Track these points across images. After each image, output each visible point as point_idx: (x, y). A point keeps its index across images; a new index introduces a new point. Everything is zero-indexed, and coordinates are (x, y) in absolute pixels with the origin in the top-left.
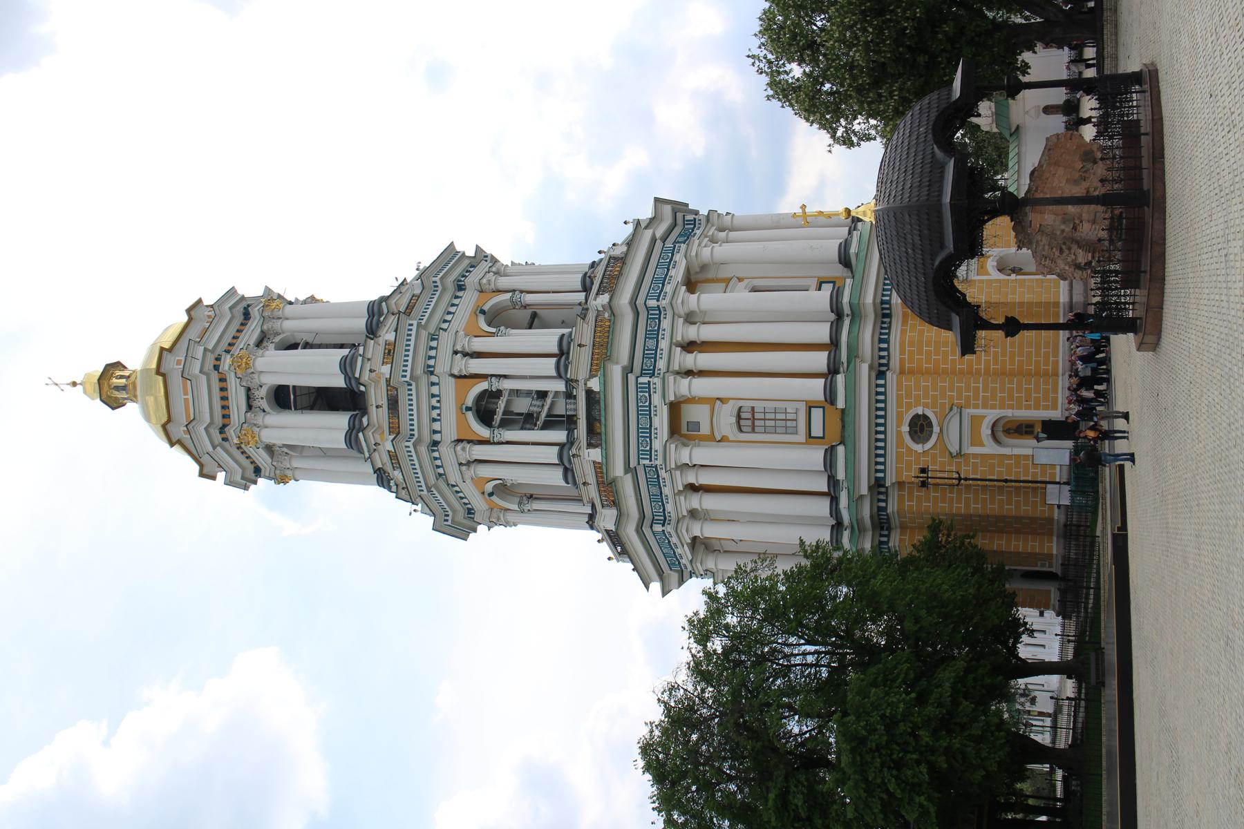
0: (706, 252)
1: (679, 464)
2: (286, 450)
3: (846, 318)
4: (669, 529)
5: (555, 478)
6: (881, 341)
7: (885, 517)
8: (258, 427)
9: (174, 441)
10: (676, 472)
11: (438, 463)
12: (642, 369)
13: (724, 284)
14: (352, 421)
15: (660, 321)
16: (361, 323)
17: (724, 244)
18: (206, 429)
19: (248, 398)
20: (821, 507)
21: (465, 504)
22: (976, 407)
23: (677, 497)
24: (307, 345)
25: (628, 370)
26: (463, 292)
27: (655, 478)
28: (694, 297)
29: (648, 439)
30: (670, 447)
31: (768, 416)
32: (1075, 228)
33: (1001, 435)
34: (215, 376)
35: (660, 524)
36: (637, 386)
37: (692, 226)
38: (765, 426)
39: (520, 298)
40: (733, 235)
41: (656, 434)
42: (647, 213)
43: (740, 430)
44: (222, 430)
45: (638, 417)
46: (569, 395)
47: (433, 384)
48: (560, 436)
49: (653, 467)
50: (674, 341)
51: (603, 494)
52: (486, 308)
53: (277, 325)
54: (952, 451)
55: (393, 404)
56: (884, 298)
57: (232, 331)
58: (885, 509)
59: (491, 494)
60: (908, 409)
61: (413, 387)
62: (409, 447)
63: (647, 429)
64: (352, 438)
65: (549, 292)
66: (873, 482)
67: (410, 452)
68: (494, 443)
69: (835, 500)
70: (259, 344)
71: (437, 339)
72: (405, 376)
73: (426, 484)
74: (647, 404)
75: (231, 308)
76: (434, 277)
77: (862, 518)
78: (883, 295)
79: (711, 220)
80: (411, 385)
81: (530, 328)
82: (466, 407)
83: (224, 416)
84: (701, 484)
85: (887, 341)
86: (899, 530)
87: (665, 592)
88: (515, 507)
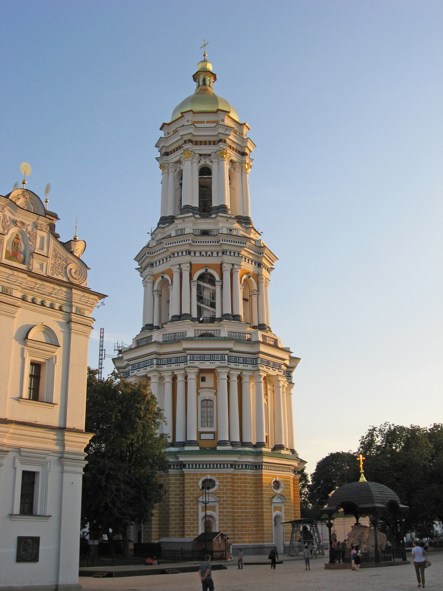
1: (188, 373)
2: (178, 170)
3: (255, 449)
4: (155, 367)
5: (174, 311)
6: (246, 465)
8: (192, 160)
10: (184, 372)
11: (180, 254)
18: (191, 133)
19: (205, 155)
21: (156, 263)
22: (219, 508)
23: (171, 371)
25: (231, 350)
26: (257, 266)
27: (179, 361)
29: (199, 359)
32: (364, 543)
35: (157, 363)
36: (224, 354)
39: (255, 294)
41: (202, 363)
44: (190, 141)
46: (213, 320)
47: (218, 253)
48: (195, 314)
49: (185, 360)
50: (243, 371)
51: (170, 335)
52: (251, 278)
54: (200, 498)
59: (162, 277)
60: (217, 478)
61: (217, 244)
62: (189, 240)
63: (204, 359)
64: (188, 208)
66: (184, 463)
69: (173, 444)
72: (222, 241)
73: (169, 247)
74: (215, 359)
80: (218, 243)
83: (196, 142)
85: (246, 468)
88: (155, 288)
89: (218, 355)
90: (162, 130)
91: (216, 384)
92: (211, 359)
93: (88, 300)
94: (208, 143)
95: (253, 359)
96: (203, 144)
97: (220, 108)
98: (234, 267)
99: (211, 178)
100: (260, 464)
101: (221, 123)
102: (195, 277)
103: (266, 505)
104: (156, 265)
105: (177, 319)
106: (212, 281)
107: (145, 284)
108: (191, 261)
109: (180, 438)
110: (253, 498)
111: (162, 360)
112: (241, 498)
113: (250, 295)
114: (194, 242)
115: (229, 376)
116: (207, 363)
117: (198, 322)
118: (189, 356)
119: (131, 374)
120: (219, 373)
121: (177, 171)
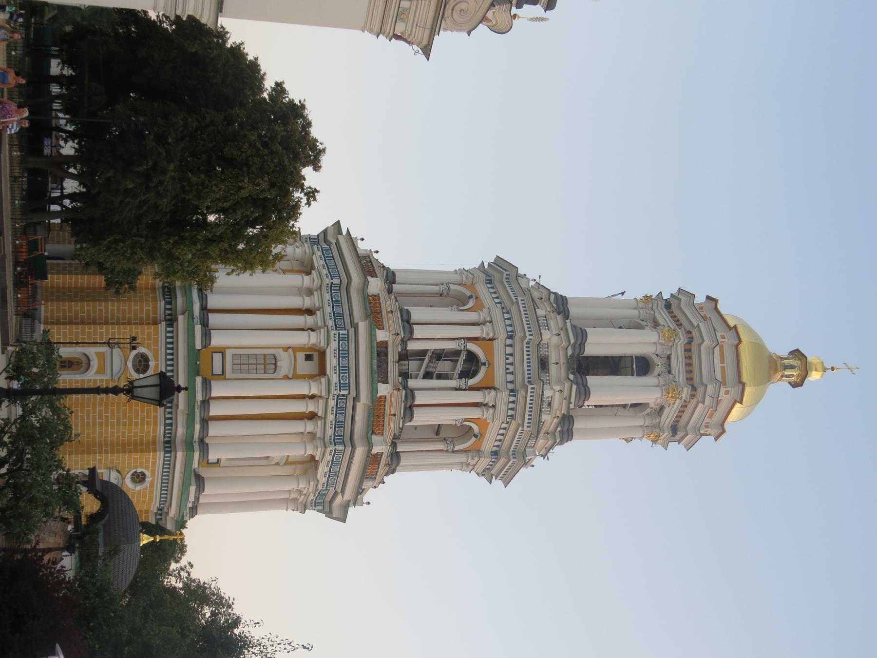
0: (302, 485)
1: (318, 331)
2: (643, 323)
3: (197, 440)
4: (327, 281)
5: (417, 314)
6: (171, 425)
7: (166, 297)
9: (733, 330)
10: (320, 325)
11: (508, 322)
12: (346, 399)
13: (289, 460)
14: (582, 351)
15: (334, 434)
16: (578, 425)
17: (292, 489)
19: (670, 365)
20: (213, 301)
21: (493, 288)
23: (321, 306)
24: (625, 406)
25: (356, 399)
28: (310, 452)
29: (341, 349)
30: (325, 344)
31: (254, 367)
33: (84, 360)
34: (696, 382)
37: (317, 501)
38: (256, 359)
39: (447, 447)
40: (286, 496)
42: (351, 509)
43: (275, 356)
44: (690, 341)
45: (348, 365)
47: (512, 382)
48: (412, 346)
50: (323, 421)
52: (473, 439)
53: (648, 422)
55: (544, 364)
56: (169, 455)
57: (686, 416)
58: (167, 303)
59: (471, 297)
61: (526, 380)
62: (530, 335)
63: (342, 357)
64: (581, 335)
65: (426, 451)
66: (175, 324)
67: (529, 331)
68: (463, 338)
69: (204, 309)
70: (662, 408)
71: (508, 416)
72: (532, 388)
73: (519, 306)
74: (341, 375)
75: (687, 435)
76: (515, 462)
77: (182, 297)
78: (170, 457)
79: (303, 506)
80: (528, 382)
81: (439, 425)
82: (485, 365)
83: (690, 350)
84: (302, 315)
85: (166, 425)
86: (157, 286)
87: (338, 224)
88: (452, 287)
89: (348, 380)
90: (707, 300)
91: (303, 377)
92: (342, 367)
93: (422, 26)
94: (689, 368)
95: (342, 437)
96: (688, 361)
97: (748, 390)
98: (491, 409)
99: (633, 375)
100: (173, 449)
101: (723, 390)
102: (472, 347)
103: (106, 459)
104: (490, 288)
105: (405, 317)
106: (466, 374)
107: (458, 272)
108: (497, 340)
109: (213, 318)
110: (118, 437)
111: (338, 293)
112: (118, 417)
113: (446, 439)
114: (529, 344)
115: (316, 398)
116: (335, 362)
117: (400, 350)
118: (345, 332)
119: (315, 247)
120: (318, 381)
121: (641, 322)
